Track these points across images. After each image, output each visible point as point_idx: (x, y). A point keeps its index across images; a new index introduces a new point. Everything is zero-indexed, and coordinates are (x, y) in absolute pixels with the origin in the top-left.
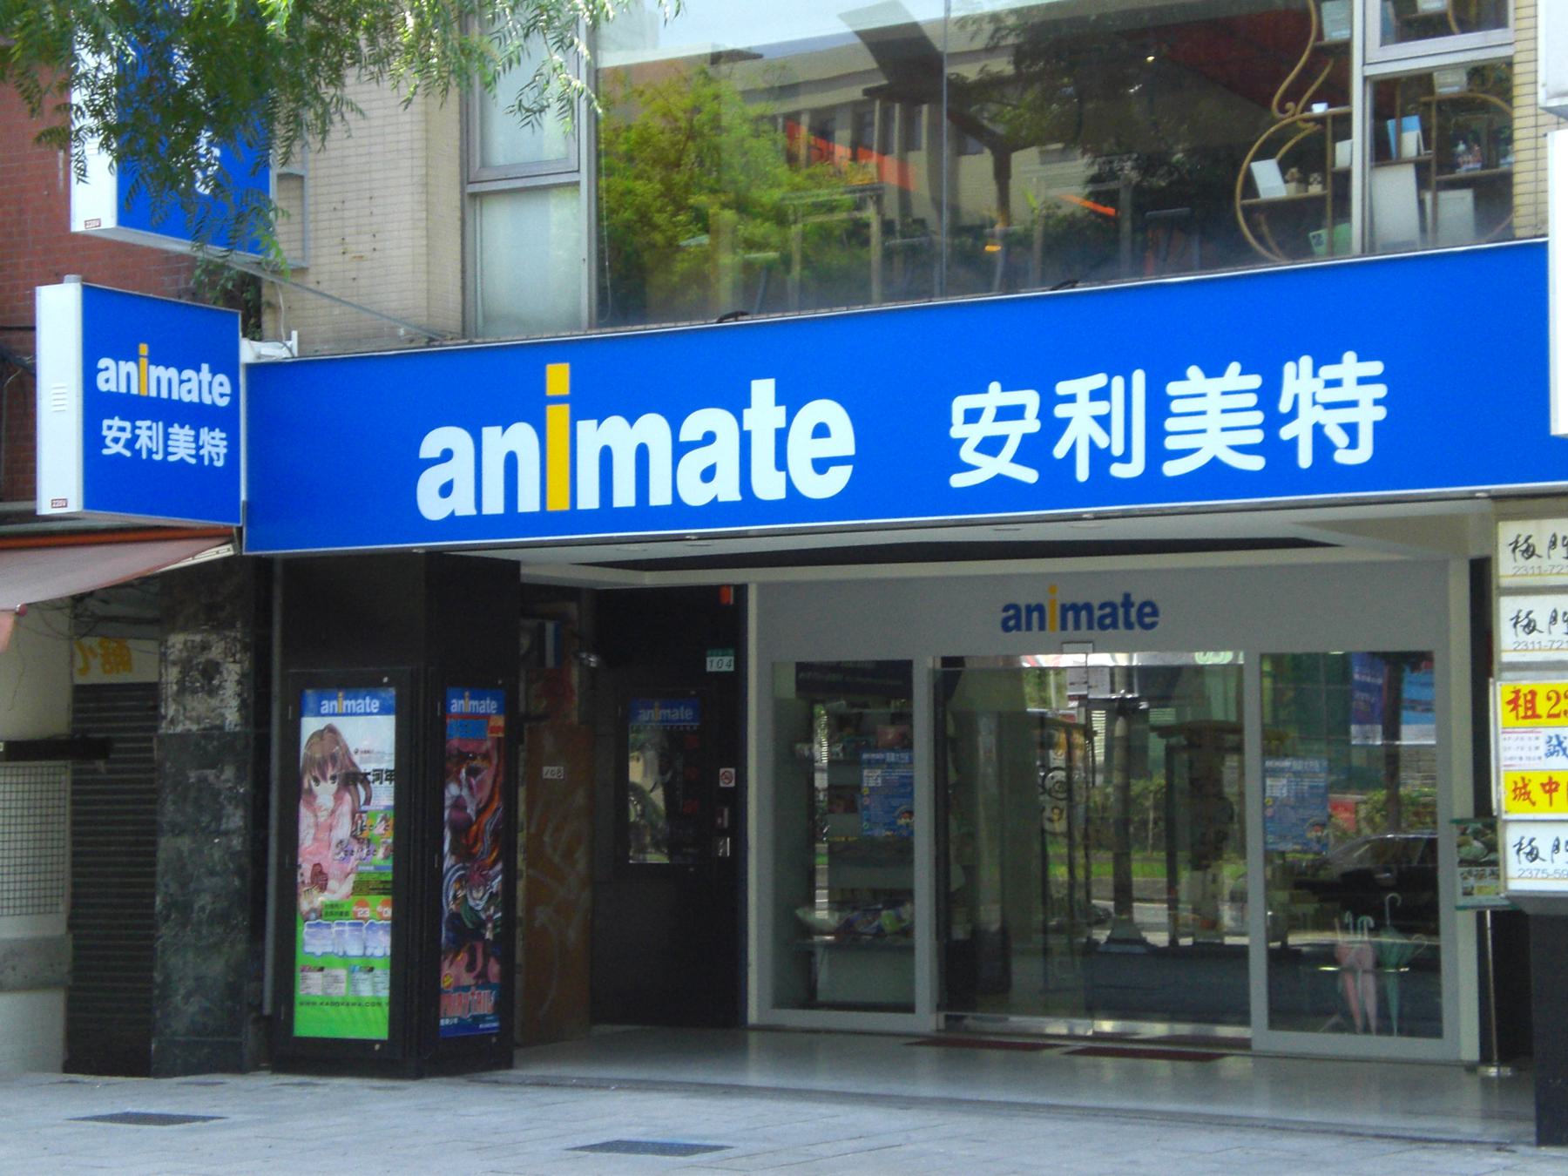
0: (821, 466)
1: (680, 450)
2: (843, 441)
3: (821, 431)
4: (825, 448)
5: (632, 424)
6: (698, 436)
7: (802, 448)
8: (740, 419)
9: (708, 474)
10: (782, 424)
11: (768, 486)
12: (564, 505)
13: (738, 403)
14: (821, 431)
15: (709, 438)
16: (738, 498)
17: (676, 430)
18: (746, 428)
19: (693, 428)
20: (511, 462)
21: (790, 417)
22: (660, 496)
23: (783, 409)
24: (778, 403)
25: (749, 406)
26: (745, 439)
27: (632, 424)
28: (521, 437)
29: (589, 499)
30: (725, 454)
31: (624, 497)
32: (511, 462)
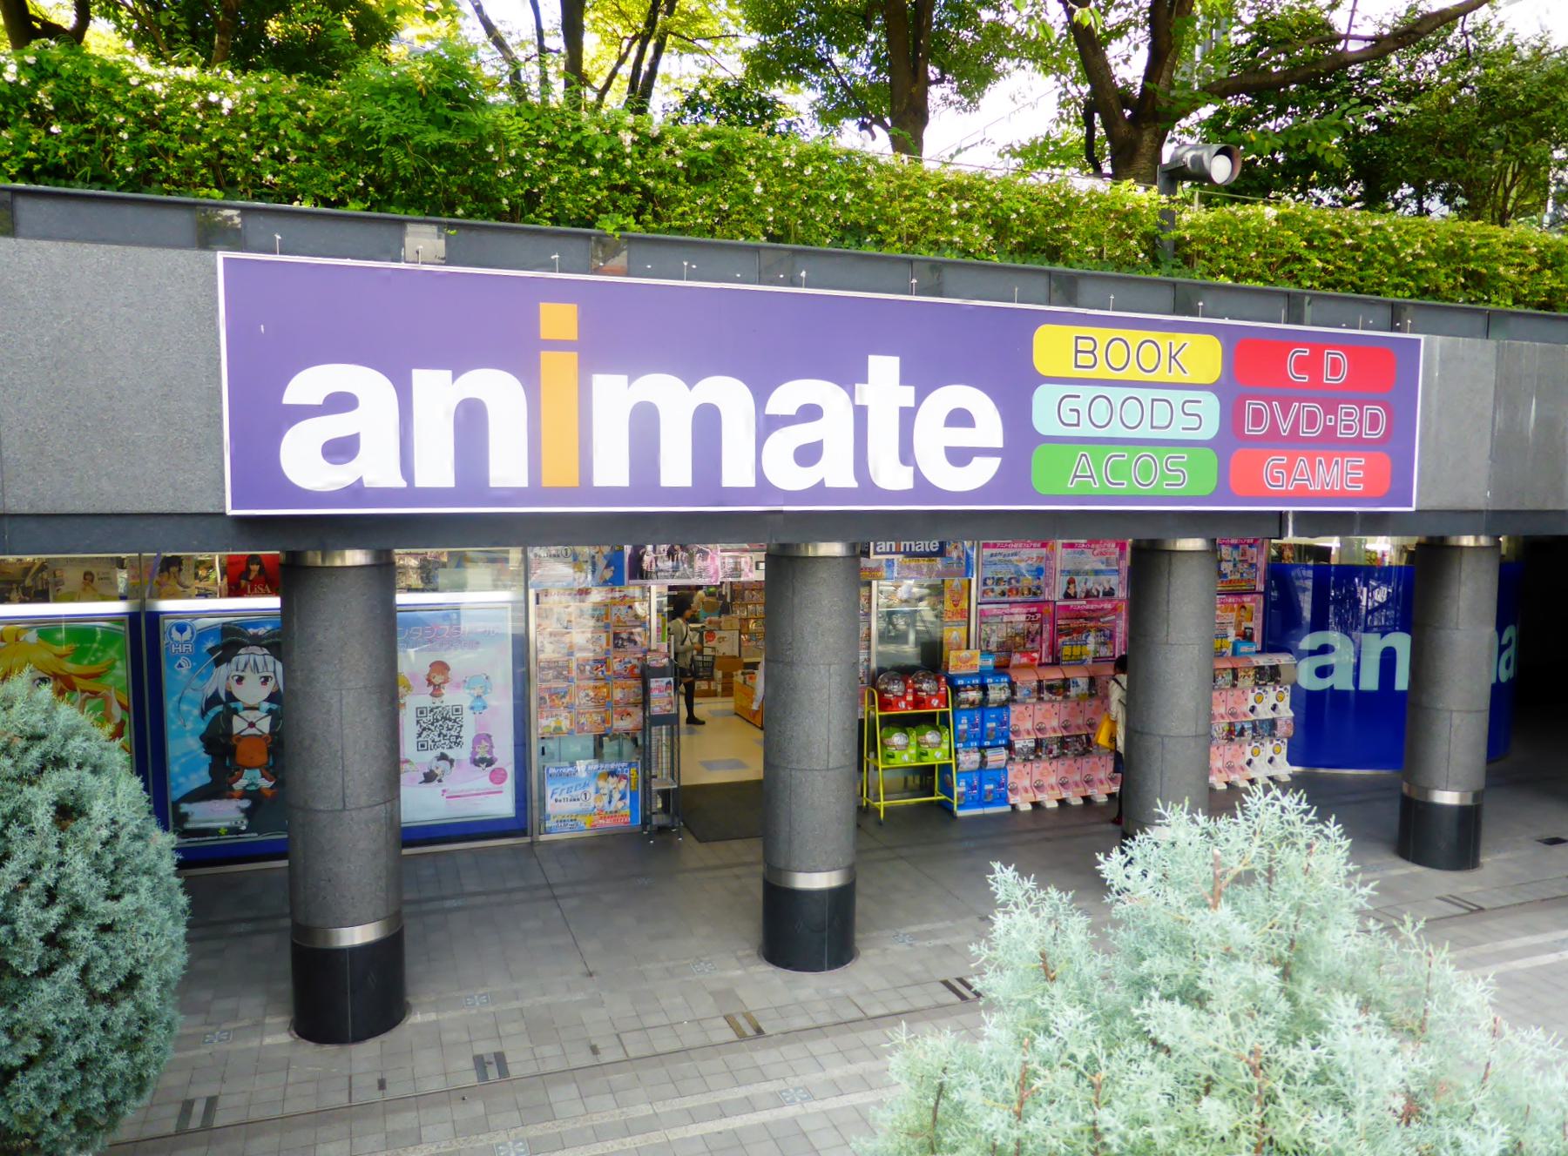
0: (959, 457)
1: (768, 425)
2: (989, 428)
3: (961, 418)
4: (962, 437)
5: (690, 387)
6: (791, 410)
7: (932, 437)
8: (852, 396)
9: (808, 455)
10: (911, 404)
11: (892, 476)
13: (850, 375)
14: (961, 418)
15: (811, 413)
16: (855, 484)
17: (761, 398)
18: (858, 402)
20: (471, 420)
21: (920, 398)
22: (736, 473)
23: (910, 391)
24: (905, 380)
25: (865, 381)
26: (861, 414)
27: (690, 387)
30: (835, 430)
31: (676, 470)
32: (471, 420)
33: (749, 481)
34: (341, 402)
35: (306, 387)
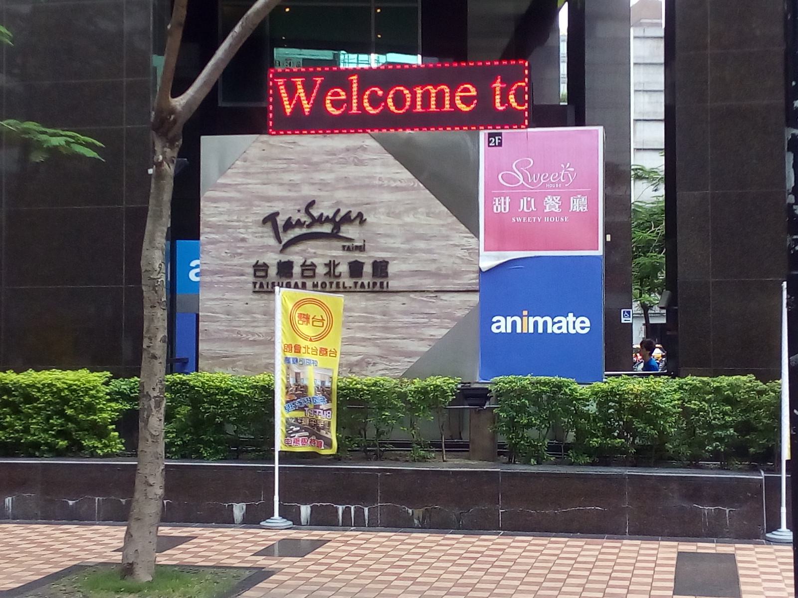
0: (583, 328)
1: (554, 323)
2: (588, 324)
3: (583, 322)
7: (578, 325)
9: (560, 328)
11: (572, 331)
12: (526, 332)
13: (566, 316)
14: (583, 322)
15: (560, 322)
16: (566, 332)
17: (553, 320)
19: (556, 320)
20: (514, 324)
22: (549, 331)
23: (575, 318)
24: (574, 316)
25: (568, 316)
26: (568, 322)
28: (517, 319)
29: (531, 331)
30: (564, 324)
31: (540, 330)
32: (514, 324)
33: (551, 332)
34: (498, 321)
35: (495, 319)
